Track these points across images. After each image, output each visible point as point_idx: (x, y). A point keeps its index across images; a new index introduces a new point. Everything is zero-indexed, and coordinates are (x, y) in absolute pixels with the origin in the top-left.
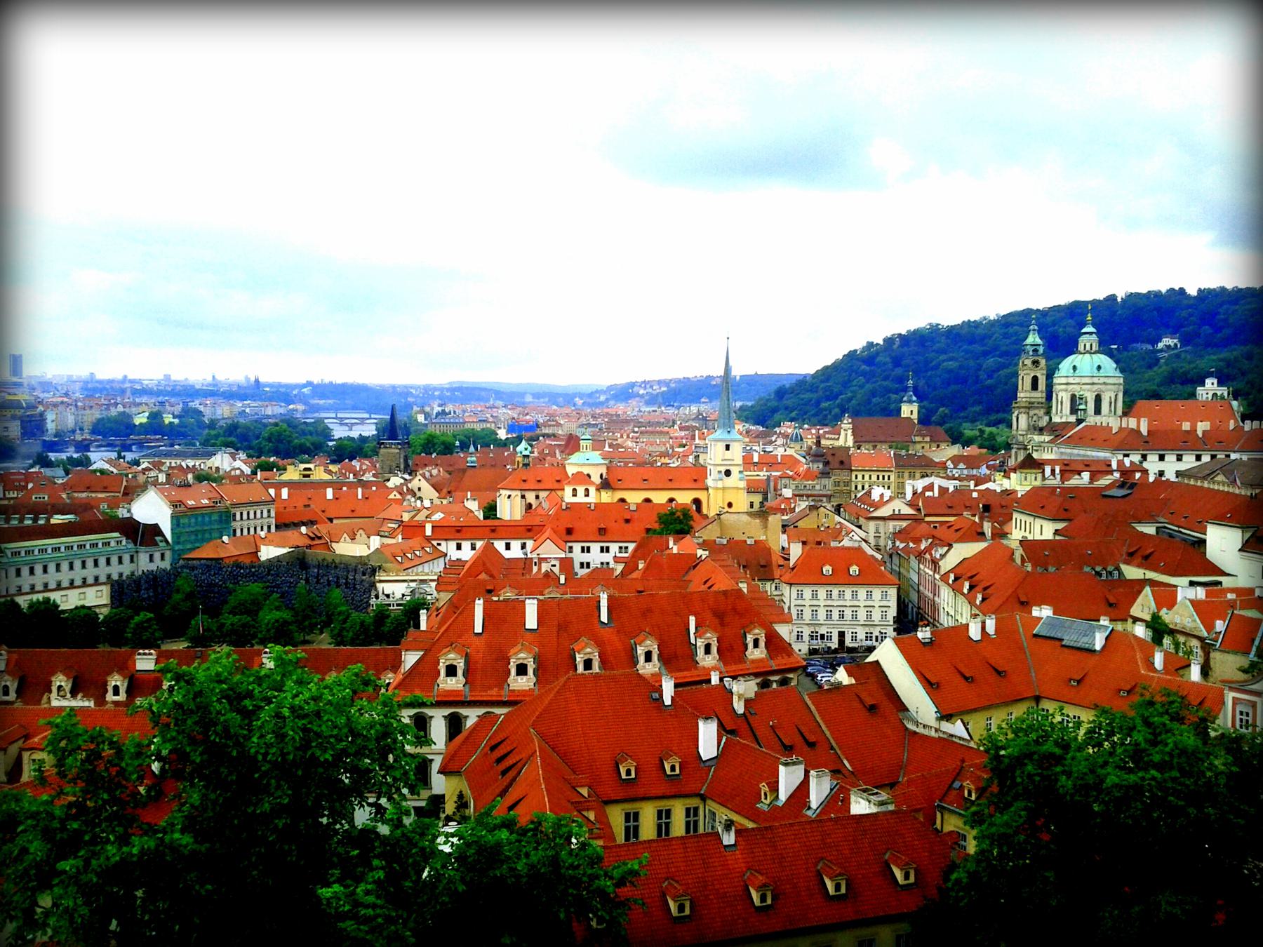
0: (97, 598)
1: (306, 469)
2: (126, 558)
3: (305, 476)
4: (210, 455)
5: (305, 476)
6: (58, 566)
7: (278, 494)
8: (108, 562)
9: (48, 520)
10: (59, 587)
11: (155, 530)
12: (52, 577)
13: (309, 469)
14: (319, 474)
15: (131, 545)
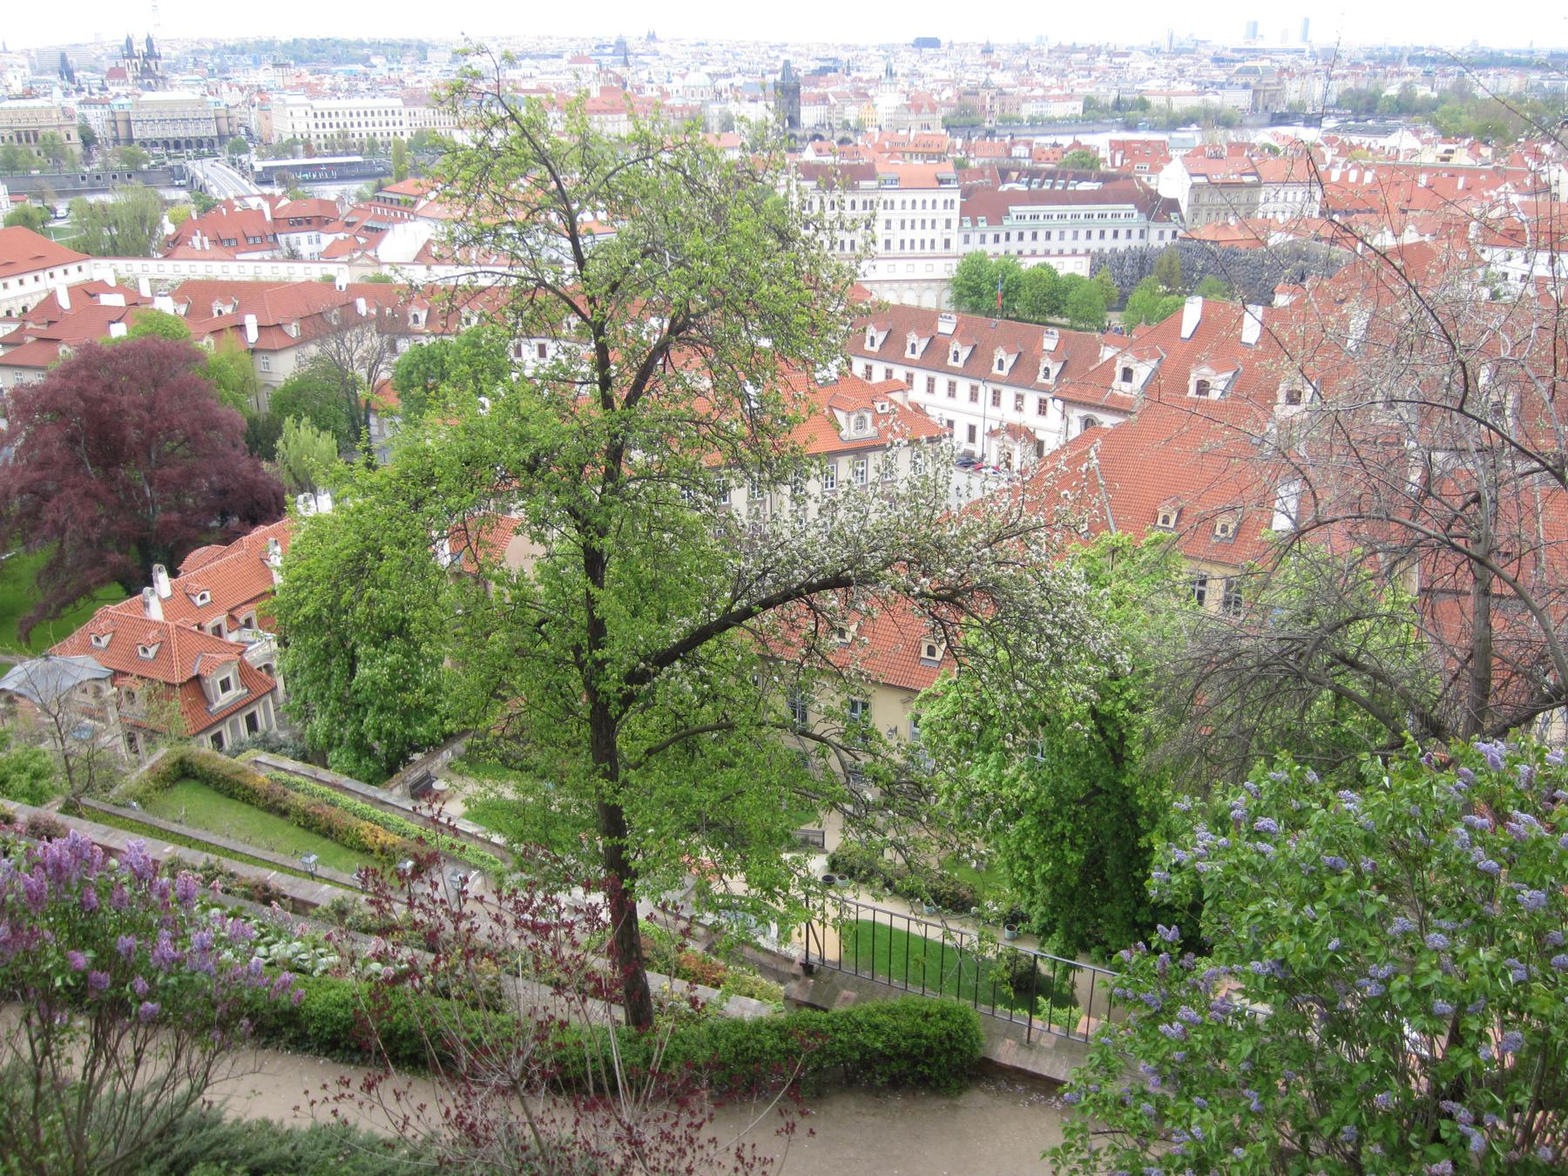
0: (1079, 267)
1: (1447, 151)
2: (1136, 233)
3: (1443, 159)
4: (1387, 132)
5: (1443, 159)
6: (1062, 233)
7: (1360, 178)
8: (1102, 234)
9: (1065, 186)
10: (1061, 253)
11: (1173, 205)
12: (1054, 244)
13: (1451, 152)
14: (1462, 158)
15: (1143, 218)
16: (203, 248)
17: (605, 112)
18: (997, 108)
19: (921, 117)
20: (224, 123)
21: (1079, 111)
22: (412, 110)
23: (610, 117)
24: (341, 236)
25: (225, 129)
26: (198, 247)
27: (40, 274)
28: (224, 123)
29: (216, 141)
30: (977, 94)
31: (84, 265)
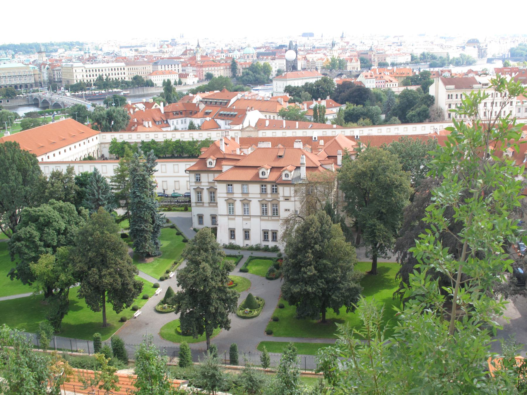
16: (149, 126)
17: (214, 66)
18: (376, 60)
19: (352, 64)
20: (37, 76)
21: (409, 60)
22: (129, 67)
23: (216, 68)
24: (208, 119)
25: (38, 80)
26: (147, 126)
27: (85, 141)
28: (37, 76)
29: (34, 85)
30: (367, 54)
31: (98, 136)
